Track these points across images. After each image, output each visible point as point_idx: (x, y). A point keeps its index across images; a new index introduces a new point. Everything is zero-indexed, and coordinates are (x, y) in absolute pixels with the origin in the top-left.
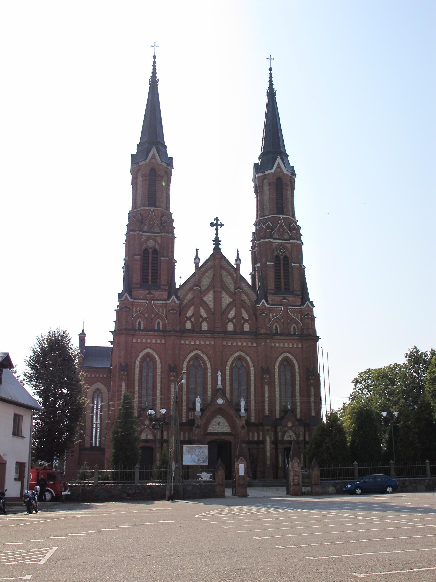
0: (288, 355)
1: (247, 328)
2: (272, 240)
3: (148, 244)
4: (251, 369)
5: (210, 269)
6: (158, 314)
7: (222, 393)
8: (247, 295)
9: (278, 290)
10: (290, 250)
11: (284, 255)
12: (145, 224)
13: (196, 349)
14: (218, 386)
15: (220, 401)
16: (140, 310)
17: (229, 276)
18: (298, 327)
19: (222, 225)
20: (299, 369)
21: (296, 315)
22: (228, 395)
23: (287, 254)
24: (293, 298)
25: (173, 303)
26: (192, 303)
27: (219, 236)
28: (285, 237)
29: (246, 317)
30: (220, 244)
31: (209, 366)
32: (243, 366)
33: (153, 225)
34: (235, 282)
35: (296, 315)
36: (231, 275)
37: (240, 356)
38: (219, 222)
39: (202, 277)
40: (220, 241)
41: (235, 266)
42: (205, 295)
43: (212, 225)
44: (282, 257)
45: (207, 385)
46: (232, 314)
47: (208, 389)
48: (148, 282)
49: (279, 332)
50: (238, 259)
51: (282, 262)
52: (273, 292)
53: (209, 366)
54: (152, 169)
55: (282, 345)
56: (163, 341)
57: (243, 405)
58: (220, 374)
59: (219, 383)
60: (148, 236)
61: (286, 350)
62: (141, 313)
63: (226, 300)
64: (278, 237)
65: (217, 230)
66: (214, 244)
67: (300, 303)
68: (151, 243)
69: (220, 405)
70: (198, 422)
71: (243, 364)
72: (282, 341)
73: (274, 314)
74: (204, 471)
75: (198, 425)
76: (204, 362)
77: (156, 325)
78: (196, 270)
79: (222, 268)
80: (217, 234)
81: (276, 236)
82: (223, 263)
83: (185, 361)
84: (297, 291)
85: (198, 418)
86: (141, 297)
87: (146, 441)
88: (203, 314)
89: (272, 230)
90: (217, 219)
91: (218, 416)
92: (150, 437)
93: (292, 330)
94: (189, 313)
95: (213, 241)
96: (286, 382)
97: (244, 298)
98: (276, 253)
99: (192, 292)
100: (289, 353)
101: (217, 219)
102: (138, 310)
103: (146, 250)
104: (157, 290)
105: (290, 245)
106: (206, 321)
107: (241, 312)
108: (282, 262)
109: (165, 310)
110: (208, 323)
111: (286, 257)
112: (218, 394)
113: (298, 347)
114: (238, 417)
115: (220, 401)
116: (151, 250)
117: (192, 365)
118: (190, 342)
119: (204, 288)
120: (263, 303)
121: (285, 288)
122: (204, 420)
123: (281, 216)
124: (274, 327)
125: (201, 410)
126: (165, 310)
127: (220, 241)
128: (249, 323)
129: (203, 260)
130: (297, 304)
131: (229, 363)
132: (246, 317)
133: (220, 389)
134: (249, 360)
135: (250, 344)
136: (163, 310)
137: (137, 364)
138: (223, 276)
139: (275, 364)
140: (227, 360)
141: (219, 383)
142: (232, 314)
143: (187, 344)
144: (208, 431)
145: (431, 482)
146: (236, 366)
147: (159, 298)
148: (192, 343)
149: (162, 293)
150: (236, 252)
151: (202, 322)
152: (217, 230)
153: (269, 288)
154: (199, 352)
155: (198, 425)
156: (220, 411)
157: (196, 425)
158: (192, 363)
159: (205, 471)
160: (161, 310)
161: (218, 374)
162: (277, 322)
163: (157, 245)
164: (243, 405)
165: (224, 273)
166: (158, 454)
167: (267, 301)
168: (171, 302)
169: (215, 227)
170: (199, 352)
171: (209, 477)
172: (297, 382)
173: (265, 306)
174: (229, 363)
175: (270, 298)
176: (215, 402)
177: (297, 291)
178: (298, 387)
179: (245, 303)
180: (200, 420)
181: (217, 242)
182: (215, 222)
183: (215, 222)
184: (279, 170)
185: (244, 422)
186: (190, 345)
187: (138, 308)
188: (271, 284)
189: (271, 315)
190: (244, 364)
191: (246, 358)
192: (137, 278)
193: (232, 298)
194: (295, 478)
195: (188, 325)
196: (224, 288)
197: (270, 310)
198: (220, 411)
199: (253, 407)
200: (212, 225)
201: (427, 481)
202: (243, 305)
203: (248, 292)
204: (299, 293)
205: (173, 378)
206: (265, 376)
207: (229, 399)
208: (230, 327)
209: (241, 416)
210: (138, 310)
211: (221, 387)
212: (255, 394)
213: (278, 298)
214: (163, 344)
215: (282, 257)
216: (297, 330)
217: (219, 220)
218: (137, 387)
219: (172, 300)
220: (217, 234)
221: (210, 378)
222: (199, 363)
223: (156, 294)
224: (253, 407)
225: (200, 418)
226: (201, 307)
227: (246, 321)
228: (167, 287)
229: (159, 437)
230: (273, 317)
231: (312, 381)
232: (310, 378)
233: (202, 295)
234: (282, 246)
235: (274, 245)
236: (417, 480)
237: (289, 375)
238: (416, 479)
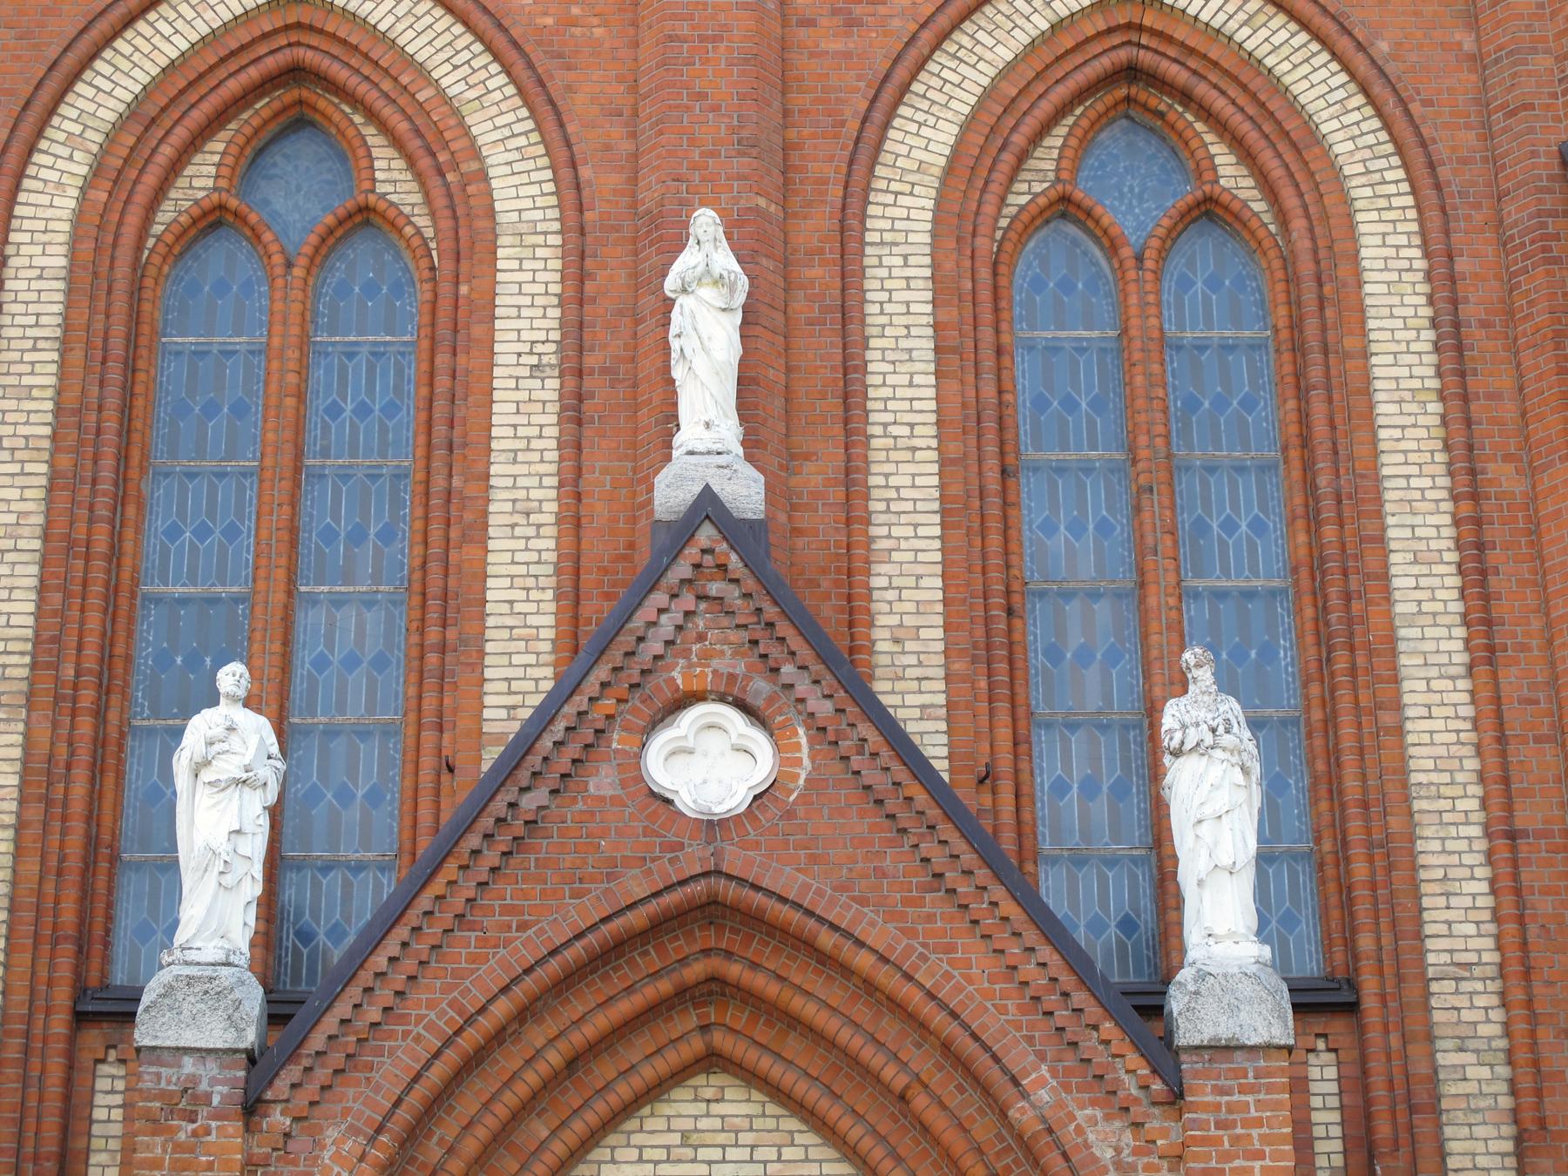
4: (1367, 223)
14: (662, 481)
22: (915, 679)
31: (520, 188)
32: (1210, 210)
45: (478, 532)
47: (496, 591)
53: (520, 188)
57: (1217, 807)
58: (725, 261)
69: (713, 827)
71: (1204, 169)
76: (440, 150)
83: (66, 122)
85: (187, 1102)
91: (682, 1108)
112: (661, 616)
114: (1131, 1073)
115: (711, 764)
117: (213, 220)
131: (925, 136)
134: (1315, 84)
140: (890, 92)
146: (1063, 207)
158: (202, 177)
161: (687, 262)
164: (1217, 807)
174: (925, 136)
176: (602, 781)
180: (226, 1137)
190: (1231, 175)
199: (1457, 916)
207: (935, 748)
209: (1186, 1035)
211: (745, 492)
212: (1486, 654)
222: (351, 158)
224: (1457, 916)
225: (251, 1108)
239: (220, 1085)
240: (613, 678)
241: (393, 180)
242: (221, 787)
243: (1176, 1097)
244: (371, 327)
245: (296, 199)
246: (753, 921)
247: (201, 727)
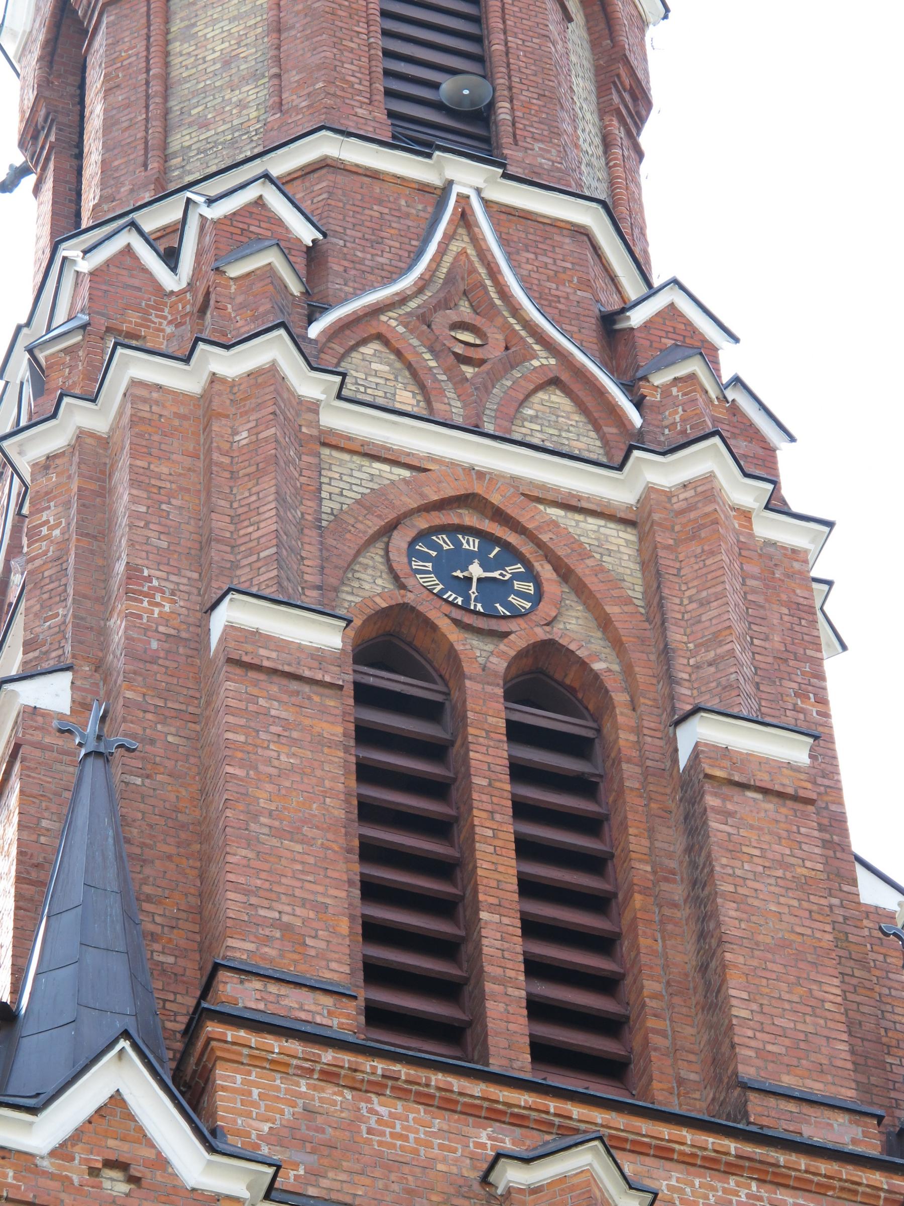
2: (310, 386)
9: (413, 1003)
10: (634, 586)
11: (522, 635)
23: (574, 628)
44: (484, 662)
105: (621, 540)
108: (487, 756)
111: (541, 679)
123: (466, 177)
167: (190, 1090)
188: (295, 897)
215: (484, 662)
234: (472, 516)
235: (348, 483)
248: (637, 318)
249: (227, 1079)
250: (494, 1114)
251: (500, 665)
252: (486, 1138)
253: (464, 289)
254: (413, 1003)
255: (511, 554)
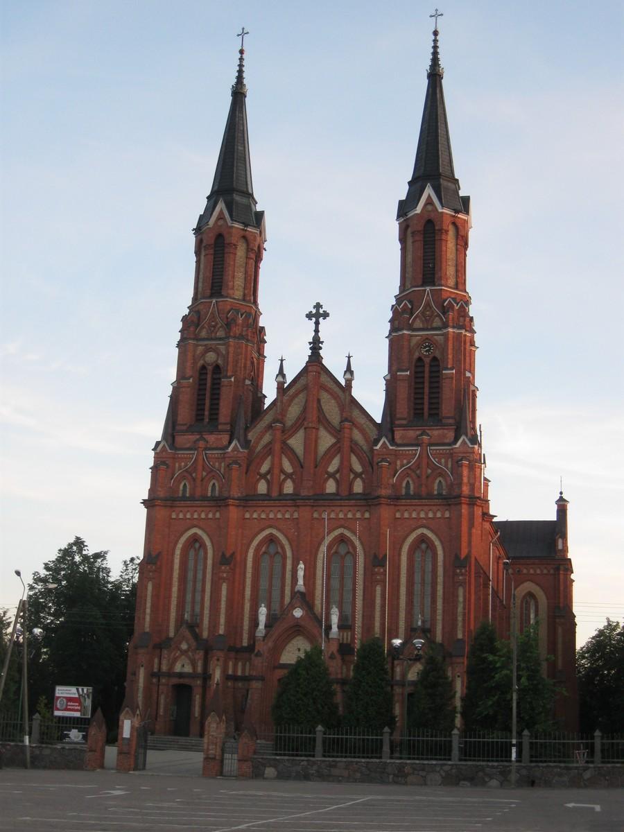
0: (425, 531)
1: (358, 487)
3: (207, 359)
5: (302, 391)
6: (212, 471)
7: (305, 599)
8: (362, 431)
12: (203, 327)
13: (270, 526)
15: (298, 613)
16: (186, 465)
17: (333, 401)
18: (446, 482)
19: (326, 315)
20: (444, 557)
21: (443, 461)
23: (438, 354)
24: (441, 431)
25: (236, 452)
26: (269, 449)
27: (320, 334)
28: (435, 325)
29: (358, 468)
30: (321, 348)
31: (289, 553)
33: (214, 327)
34: (342, 408)
35: (443, 461)
36: (334, 396)
37: (342, 535)
38: (321, 311)
39: (289, 406)
40: (322, 342)
41: (343, 382)
42: (291, 436)
43: (309, 316)
44: (427, 360)
46: (333, 466)
48: (203, 419)
49: (412, 493)
50: (349, 370)
51: (427, 369)
52: (404, 422)
53: (289, 553)
54: (229, 235)
55: (414, 515)
56: (218, 515)
59: (301, 582)
60: (205, 345)
61: (422, 522)
62: (186, 471)
63: (326, 441)
64: (421, 326)
65: (317, 323)
66: (311, 348)
67: (452, 439)
68: (211, 357)
69: (297, 618)
70: (260, 647)
72: (414, 507)
73: (405, 462)
74: (73, 728)
75: (259, 651)
76: (283, 547)
77: (210, 489)
78: (278, 392)
79: (323, 387)
80: (317, 331)
81: (418, 324)
82: (324, 378)
84: (449, 418)
85: (260, 640)
86: (188, 446)
87: (181, 675)
88: (287, 467)
89: (412, 314)
90: (318, 306)
92: (188, 669)
93: (436, 488)
94: (265, 468)
95: (310, 343)
96: (423, 580)
97: (357, 436)
98: (417, 355)
99: (270, 432)
100: (428, 528)
101: (318, 306)
102: (182, 467)
103: (204, 367)
104: (211, 433)
106: (291, 478)
107: (349, 461)
109: (223, 465)
110: (294, 481)
111: (435, 359)
113: (443, 517)
115: (298, 613)
116: (210, 368)
117: (265, 553)
118: (259, 515)
119: (289, 423)
120: (384, 442)
121: (430, 415)
122: (270, 644)
124: (404, 485)
125: (266, 626)
126: (223, 465)
127: (322, 342)
128: (362, 478)
129: (290, 378)
130: (447, 441)
132: (358, 468)
133: (298, 591)
135: (358, 515)
136: (220, 464)
137: (178, 552)
138: (322, 401)
139: (401, 548)
141: (301, 582)
142: (333, 466)
143: (256, 518)
144: (281, 662)
145: (454, 771)
146: (336, 552)
147: (214, 446)
148: (263, 516)
149: (219, 436)
150: (347, 358)
151: (284, 480)
152: (317, 323)
153: (398, 416)
154: (274, 532)
155: (259, 651)
156: (297, 629)
157: (256, 651)
158: (264, 549)
159: (76, 728)
160: (217, 464)
162: (408, 475)
163: (219, 359)
165: (325, 396)
166: (198, 697)
168: (232, 451)
169: (314, 319)
170: (274, 532)
171: (81, 737)
172: (440, 579)
173: (386, 447)
175: (398, 434)
177: (449, 418)
178: (440, 588)
179: (356, 444)
181: (316, 345)
182: (314, 311)
183: (314, 311)
184: (429, 208)
185: (334, 648)
186: (260, 519)
187: (183, 464)
189: (398, 462)
191: (352, 538)
192: (185, 414)
193: (335, 437)
194: (210, 747)
195: (262, 487)
196: (323, 420)
197: (396, 455)
198: (297, 629)
200: (309, 316)
201: (446, 768)
202: (354, 448)
203: (364, 426)
204: (451, 421)
205: (225, 575)
206: (376, 570)
208: (331, 487)
210: (182, 467)
213: (412, 434)
214: (216, 519)
215: (427, 360)
216: (444, 487)
217: (321, 307)
218: (175, 589)
219: (234, 448)
220: (317, 331)
221: (290, 573)
223: (211, 438)
225: (264, 640)
226: (283, 456)
227: (357, 475)
228: (228, 427)
229: (199, 669)
230: (402, 466)
231: (461, 578)
232: (458, 571)
233: (287, 436)
235: (414, 341)
236: (428, 764)
237: (429, 567)
238: (426, 762)
239: (261, 639)
240: (292, 607)
241: (280, 550)
242: (263, 611)
243: (329, 642)
244: (278, 559)
245: (272, 550)
246: (300, 627)
247: (261, 609)
248: (445, 304)
249: (396, 433)
250: (419, 430)
251: (428, 361)
252: (418, 433)
253: (428, 305)
254: (417, 413)
255: (431, 344)
